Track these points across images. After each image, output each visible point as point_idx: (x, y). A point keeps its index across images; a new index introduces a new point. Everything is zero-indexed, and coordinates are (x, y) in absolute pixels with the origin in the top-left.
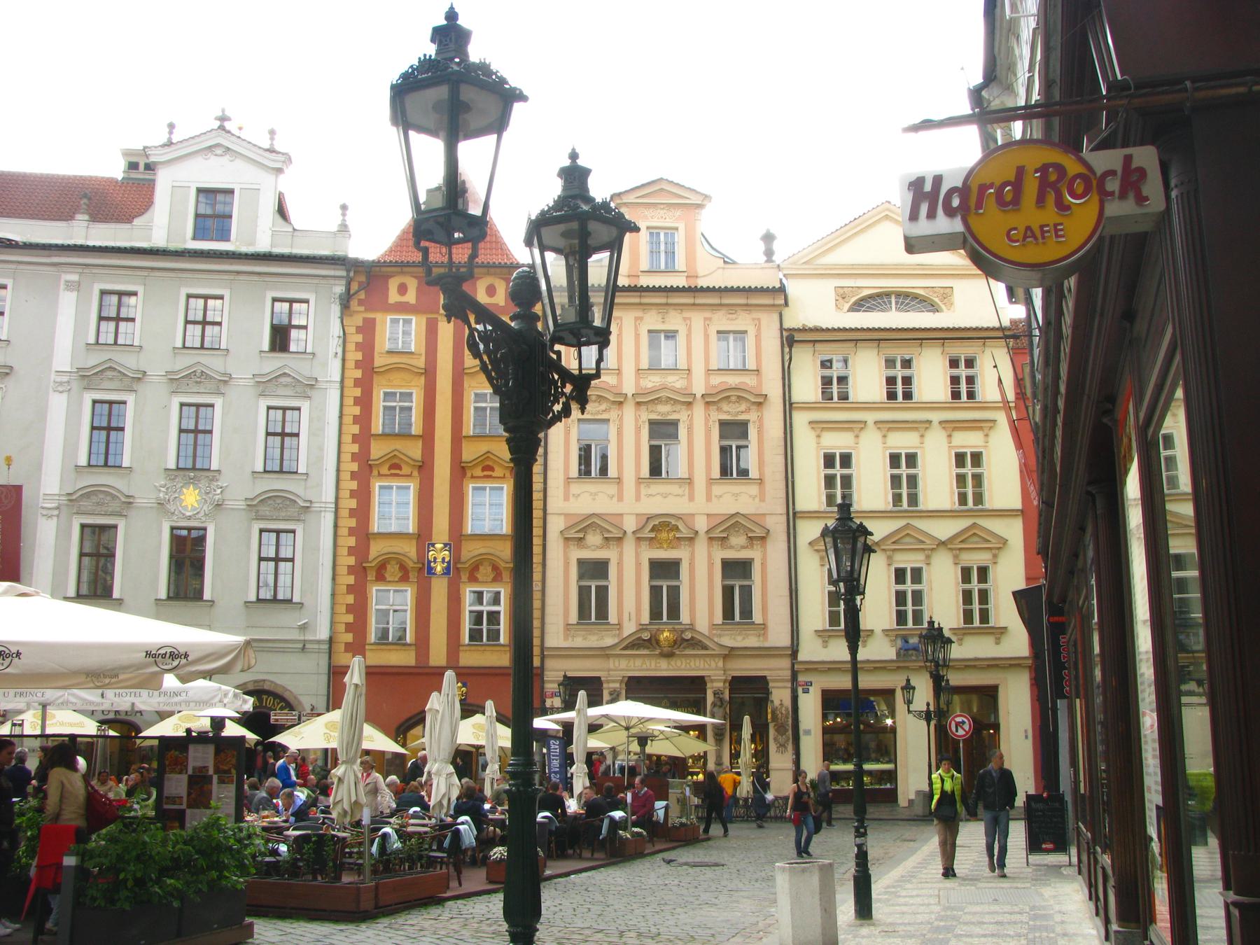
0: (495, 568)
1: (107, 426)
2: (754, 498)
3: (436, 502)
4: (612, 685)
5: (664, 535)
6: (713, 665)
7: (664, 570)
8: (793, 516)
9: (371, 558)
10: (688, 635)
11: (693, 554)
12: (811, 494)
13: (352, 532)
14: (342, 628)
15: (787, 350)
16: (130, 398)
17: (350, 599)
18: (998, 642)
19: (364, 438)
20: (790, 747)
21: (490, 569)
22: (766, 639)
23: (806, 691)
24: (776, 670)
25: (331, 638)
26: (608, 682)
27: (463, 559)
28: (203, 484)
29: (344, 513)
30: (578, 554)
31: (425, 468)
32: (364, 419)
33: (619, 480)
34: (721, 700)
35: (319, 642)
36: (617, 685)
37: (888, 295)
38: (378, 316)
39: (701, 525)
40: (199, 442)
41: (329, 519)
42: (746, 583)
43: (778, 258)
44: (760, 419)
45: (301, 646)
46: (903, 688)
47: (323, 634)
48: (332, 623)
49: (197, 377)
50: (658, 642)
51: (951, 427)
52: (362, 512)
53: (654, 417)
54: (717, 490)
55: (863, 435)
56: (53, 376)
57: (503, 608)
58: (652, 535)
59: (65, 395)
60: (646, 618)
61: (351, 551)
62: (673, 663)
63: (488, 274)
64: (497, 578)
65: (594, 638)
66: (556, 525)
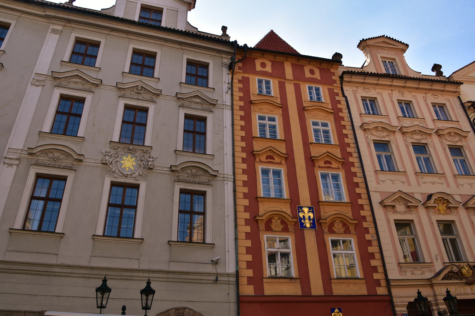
1: (69, 113)
3: (299, 180)
9: (260, 214)
13: (245, 196)
14: (243, 265)
16: (89, 97)
17: (249, 243)
19: (249, 138)
21: (341, 224)
25: (237, 272)
28: (139, 153)
29: (239, 183)
30: (393, 217)
31: (289, 158)
32: (247, 128)
35: (228, 275)
38: (251, 77)
41: (229, 186)
45: (214, 278)
47: (231, 269)
48: (237, 262)
49: (140, 90)
52: (251, 183)
54: (461, 180)
56: (33, 76)
59: (40, 88)
61: (246, 209)
65: (418, 272)
66: (376, 198)
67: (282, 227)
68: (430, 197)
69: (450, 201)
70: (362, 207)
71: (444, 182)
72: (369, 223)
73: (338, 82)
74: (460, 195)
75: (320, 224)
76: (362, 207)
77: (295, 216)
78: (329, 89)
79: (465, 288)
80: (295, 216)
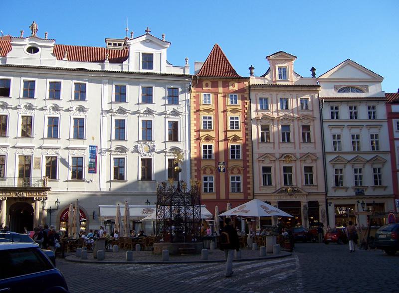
0: (239, 170)
5: (287, 159)
7: (287, 170)
8: (324, 153)
12: (329, 147)
15: (321, 104)
18: (385, 190)
23: (330, 205)
24: (321, 199)
27: (229, 167)
33: (274, 143)
34: (306, 208)
37: (349, 87)
39: (298, 156)
40: (121, 131)
43: (317, 76)
44: (314, 125)
46: (362, 204)
51: (370, 127)
53: (283, 124)
54: (302, 146)
55: (344, 129)
57: (241, 181)
58: (285, 159)
60: (283, 184)
63: (233, 80)
64: (239, 173)
66: (256, 156)
67: (210, 172)
68: (283, 155)
70: (248, 161)
73: (248, 91)
75: (227, 170)
76: (248, 161)
77: (217, 167)
78: (242, 95)
80: (217, 167)
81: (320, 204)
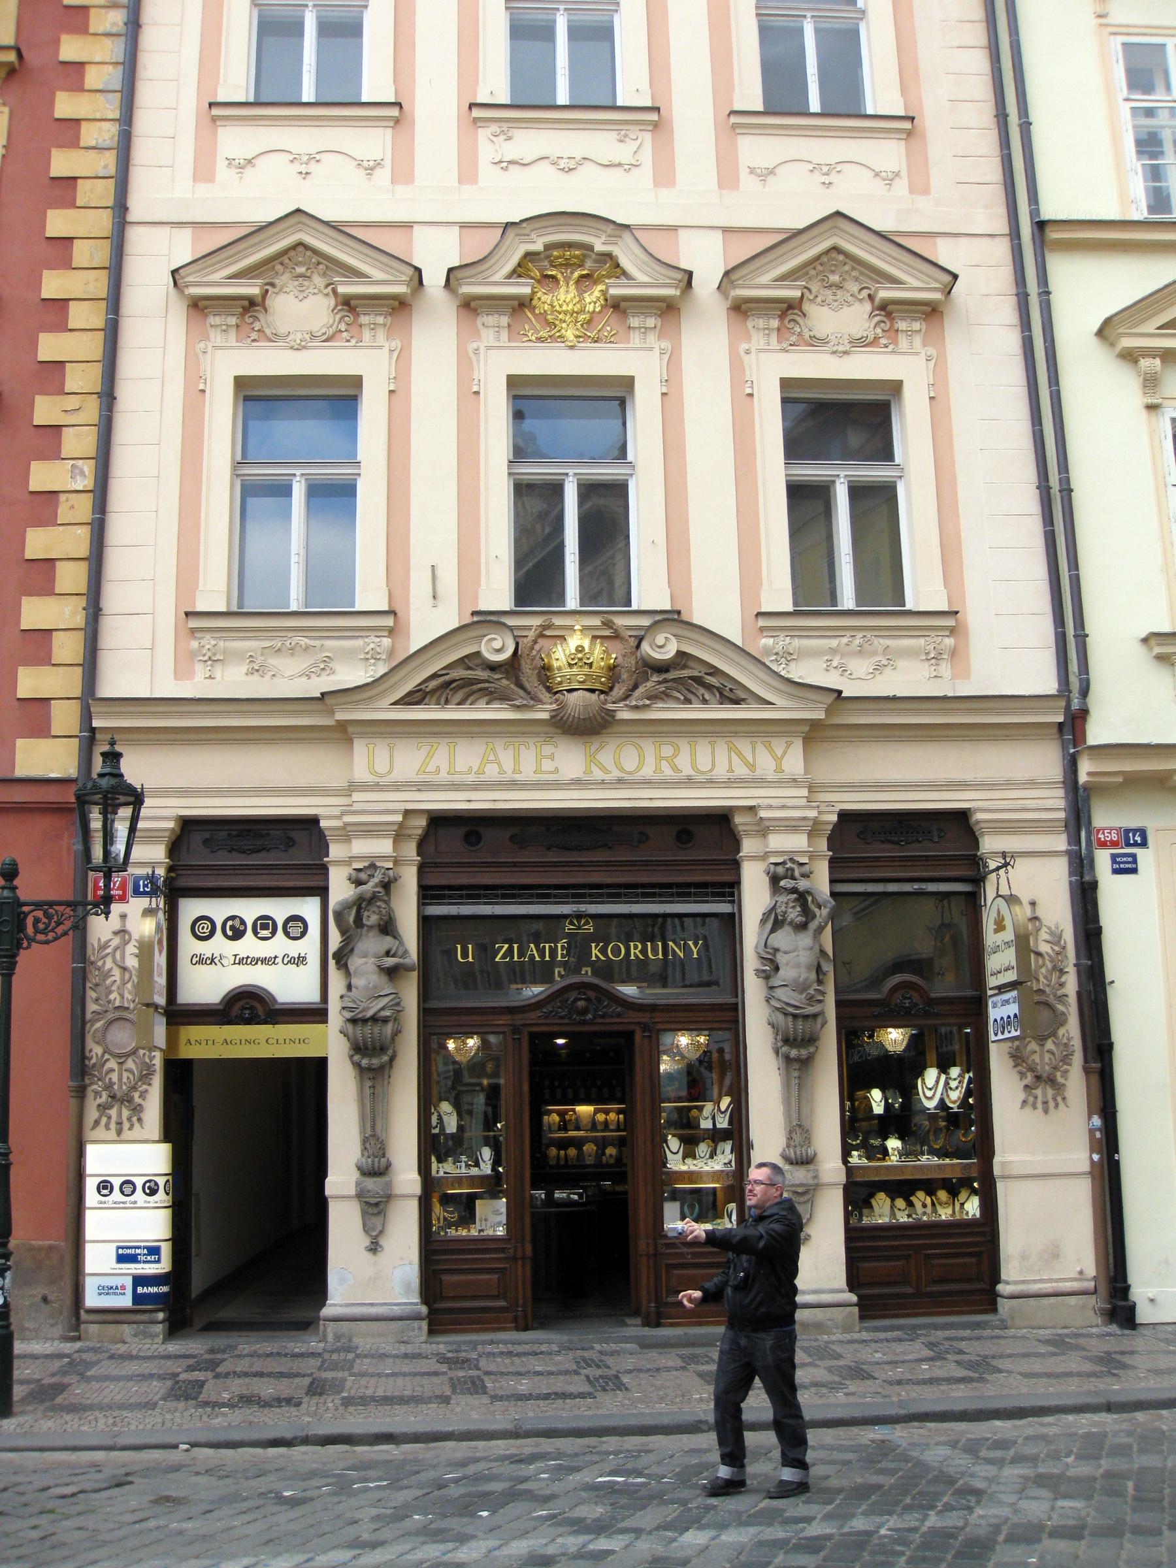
2: (890, 179)
4: (363, 847)
5: (565, 296)
6: (765, 763)
10: (663, 646)
11: (673, 362)
20: (1076, 1083)
22: (962, 669)
24: (1006, 788)
26: (347, 833)
33: (396, 113)
34: (802, 897)
36: (383, 847)
39: (706, 259)
42: (874, 473)
50: (545, 672)
62: (606, 756)
69: (624, 262)
71: (646, 156)
72: (72, 402)
74: (726, 230)
79: (548, 749)
81: (989, 844)
